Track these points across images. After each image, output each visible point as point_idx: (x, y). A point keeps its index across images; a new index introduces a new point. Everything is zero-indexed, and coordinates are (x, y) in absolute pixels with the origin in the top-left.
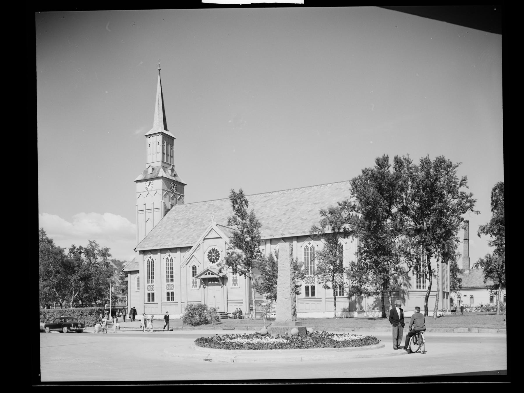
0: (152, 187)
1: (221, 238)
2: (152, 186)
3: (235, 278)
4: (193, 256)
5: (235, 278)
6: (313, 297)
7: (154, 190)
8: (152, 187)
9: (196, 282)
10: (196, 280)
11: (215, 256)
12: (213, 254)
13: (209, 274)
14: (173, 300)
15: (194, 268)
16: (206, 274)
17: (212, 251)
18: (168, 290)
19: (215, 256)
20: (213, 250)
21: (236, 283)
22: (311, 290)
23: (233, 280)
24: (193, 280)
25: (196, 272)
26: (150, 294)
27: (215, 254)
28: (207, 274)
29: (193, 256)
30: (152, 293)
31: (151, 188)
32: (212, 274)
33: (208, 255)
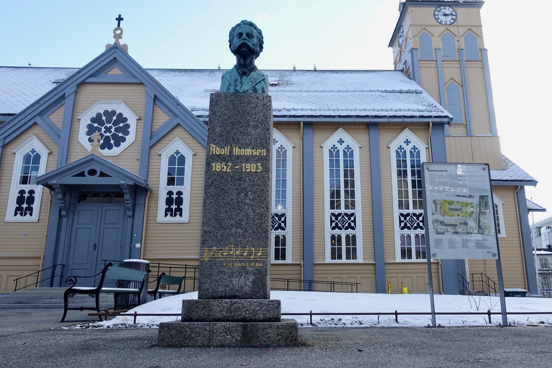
1: (141, 84)
3: (175, 196)
4: (35, 123)
5: (175, 196)
6: (351, 261)
9: (31, 200)
10: (32, 192)
11: (113, 130)
13: (92, 172)
16: (82, 174)
20: (109, 114)
21: (179, 211)
22: (347, 243)
23: (169, 201)
27: (114, 124)
28: (86, 174)
29: (35, 123)
32: (102, 175)
33: (89, 126)
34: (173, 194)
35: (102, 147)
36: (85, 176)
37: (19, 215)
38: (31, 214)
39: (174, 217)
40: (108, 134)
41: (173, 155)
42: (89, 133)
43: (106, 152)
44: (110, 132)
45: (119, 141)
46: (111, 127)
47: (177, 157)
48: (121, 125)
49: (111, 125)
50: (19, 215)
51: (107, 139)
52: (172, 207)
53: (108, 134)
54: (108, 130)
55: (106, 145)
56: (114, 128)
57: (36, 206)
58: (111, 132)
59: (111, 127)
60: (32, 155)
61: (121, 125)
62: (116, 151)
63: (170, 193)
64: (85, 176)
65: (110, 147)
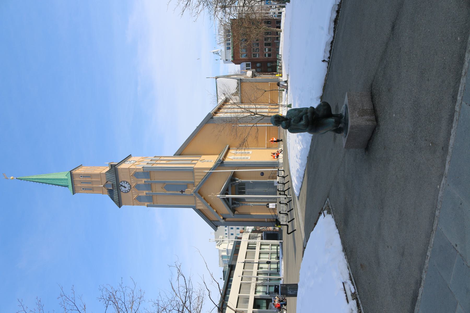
0: (126, 183)
2: (125, 182)
8: (127, 182)
31: (128, 184)
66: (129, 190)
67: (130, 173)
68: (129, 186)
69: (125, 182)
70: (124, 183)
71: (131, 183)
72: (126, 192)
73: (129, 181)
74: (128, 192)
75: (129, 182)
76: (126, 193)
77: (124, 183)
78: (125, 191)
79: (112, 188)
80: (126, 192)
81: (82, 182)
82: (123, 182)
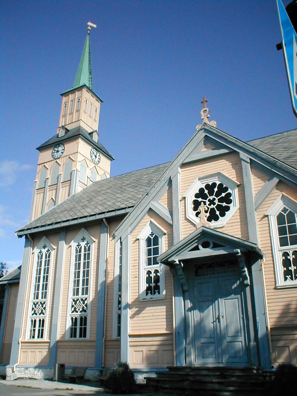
0: (62, 153)
2: (63, 151)
7: (65, 156)
11: (216, 201)
12: (211, 198)
14: (85, 336)
15: (153, 241)
16: (196, 248)
17: (206, 192)
18: (75, 313)
19: (216, 201)
24: (149, 273)
25: (156, 251)
26: (35, 321)
27: (216, 196)
28: (200, 247)
30: (40, 320)
34: (289, 255)
35: (209, 219)
36: (198, 249)
37: (149, 294)
38: (159, 293)
39: (295, 280)
40: (212, 206)
41: (280, 214)
42: (195, 209)
43: (213, 224)
44: (214, 204)
45: (223, 211)
46: (214, 199)
47: (285, 215)
48: (223, 195)
49: (214, 197)
50: (149, 294)
51: (212, 211)
52: (290, 268)
53: (212, 206)
54: (212, 202)
55: (213, 217)
56: (217, 199)
57: (161, 284)
58: (215, 203)
59: (214, 199)
60: (152, 238)
61: (223, 195)
62: (222, 221)
63: (286, 254)
64: (198, 249)
65: (216, 219)
66: (54, 157)
67: (71, 154)
68: (59, 157)
69: (63, 151)
70: (63, 150)
71: (61, 158)
72: (53, 154)
73: (64, 154)
74: (53, 156)
75: (63, 155)
76: (52, 153)
77: (63, 150)
78: (54, 153)
79: (59, 136)
80: (53, 154)
81: (74, 101)
82: (63, 148)
